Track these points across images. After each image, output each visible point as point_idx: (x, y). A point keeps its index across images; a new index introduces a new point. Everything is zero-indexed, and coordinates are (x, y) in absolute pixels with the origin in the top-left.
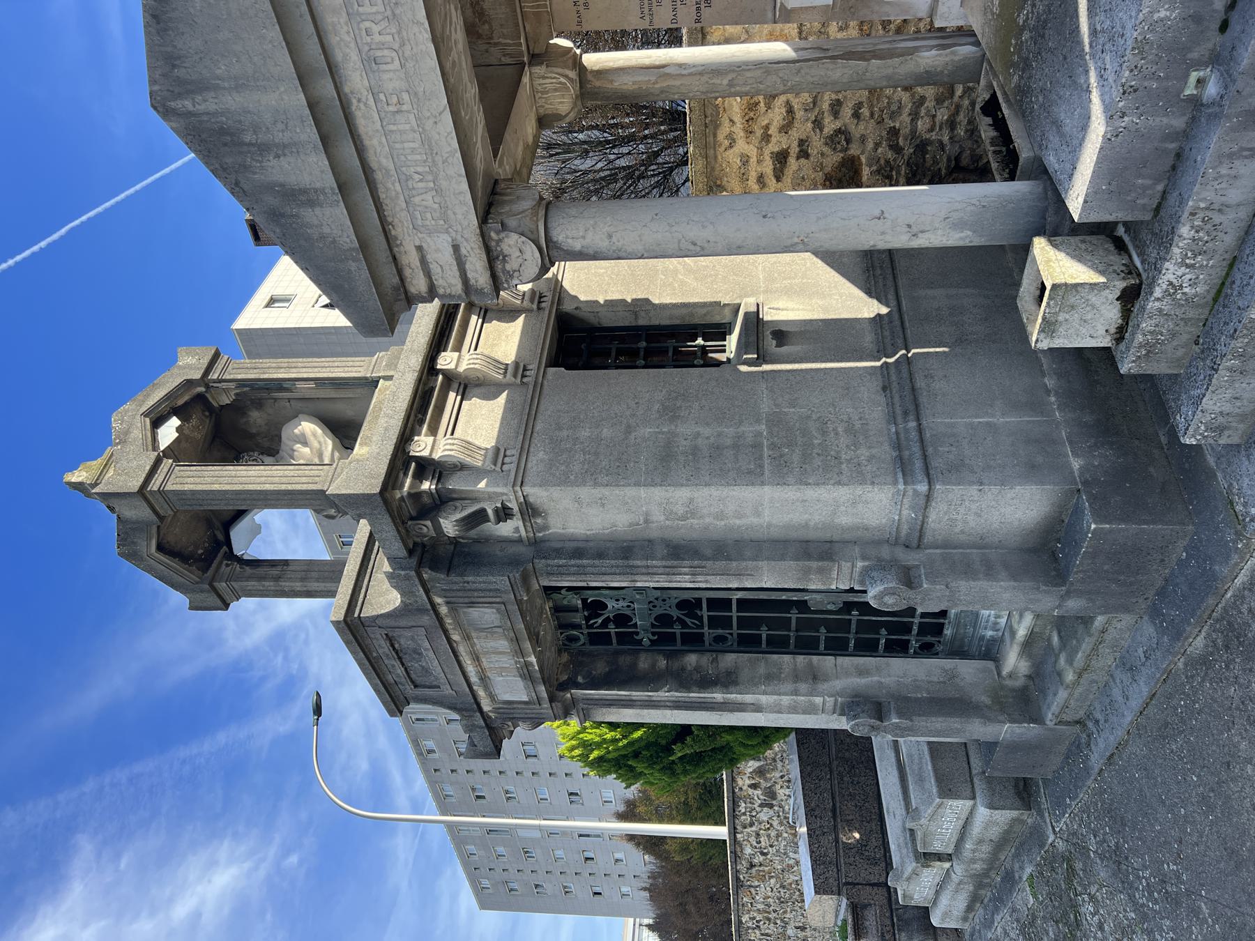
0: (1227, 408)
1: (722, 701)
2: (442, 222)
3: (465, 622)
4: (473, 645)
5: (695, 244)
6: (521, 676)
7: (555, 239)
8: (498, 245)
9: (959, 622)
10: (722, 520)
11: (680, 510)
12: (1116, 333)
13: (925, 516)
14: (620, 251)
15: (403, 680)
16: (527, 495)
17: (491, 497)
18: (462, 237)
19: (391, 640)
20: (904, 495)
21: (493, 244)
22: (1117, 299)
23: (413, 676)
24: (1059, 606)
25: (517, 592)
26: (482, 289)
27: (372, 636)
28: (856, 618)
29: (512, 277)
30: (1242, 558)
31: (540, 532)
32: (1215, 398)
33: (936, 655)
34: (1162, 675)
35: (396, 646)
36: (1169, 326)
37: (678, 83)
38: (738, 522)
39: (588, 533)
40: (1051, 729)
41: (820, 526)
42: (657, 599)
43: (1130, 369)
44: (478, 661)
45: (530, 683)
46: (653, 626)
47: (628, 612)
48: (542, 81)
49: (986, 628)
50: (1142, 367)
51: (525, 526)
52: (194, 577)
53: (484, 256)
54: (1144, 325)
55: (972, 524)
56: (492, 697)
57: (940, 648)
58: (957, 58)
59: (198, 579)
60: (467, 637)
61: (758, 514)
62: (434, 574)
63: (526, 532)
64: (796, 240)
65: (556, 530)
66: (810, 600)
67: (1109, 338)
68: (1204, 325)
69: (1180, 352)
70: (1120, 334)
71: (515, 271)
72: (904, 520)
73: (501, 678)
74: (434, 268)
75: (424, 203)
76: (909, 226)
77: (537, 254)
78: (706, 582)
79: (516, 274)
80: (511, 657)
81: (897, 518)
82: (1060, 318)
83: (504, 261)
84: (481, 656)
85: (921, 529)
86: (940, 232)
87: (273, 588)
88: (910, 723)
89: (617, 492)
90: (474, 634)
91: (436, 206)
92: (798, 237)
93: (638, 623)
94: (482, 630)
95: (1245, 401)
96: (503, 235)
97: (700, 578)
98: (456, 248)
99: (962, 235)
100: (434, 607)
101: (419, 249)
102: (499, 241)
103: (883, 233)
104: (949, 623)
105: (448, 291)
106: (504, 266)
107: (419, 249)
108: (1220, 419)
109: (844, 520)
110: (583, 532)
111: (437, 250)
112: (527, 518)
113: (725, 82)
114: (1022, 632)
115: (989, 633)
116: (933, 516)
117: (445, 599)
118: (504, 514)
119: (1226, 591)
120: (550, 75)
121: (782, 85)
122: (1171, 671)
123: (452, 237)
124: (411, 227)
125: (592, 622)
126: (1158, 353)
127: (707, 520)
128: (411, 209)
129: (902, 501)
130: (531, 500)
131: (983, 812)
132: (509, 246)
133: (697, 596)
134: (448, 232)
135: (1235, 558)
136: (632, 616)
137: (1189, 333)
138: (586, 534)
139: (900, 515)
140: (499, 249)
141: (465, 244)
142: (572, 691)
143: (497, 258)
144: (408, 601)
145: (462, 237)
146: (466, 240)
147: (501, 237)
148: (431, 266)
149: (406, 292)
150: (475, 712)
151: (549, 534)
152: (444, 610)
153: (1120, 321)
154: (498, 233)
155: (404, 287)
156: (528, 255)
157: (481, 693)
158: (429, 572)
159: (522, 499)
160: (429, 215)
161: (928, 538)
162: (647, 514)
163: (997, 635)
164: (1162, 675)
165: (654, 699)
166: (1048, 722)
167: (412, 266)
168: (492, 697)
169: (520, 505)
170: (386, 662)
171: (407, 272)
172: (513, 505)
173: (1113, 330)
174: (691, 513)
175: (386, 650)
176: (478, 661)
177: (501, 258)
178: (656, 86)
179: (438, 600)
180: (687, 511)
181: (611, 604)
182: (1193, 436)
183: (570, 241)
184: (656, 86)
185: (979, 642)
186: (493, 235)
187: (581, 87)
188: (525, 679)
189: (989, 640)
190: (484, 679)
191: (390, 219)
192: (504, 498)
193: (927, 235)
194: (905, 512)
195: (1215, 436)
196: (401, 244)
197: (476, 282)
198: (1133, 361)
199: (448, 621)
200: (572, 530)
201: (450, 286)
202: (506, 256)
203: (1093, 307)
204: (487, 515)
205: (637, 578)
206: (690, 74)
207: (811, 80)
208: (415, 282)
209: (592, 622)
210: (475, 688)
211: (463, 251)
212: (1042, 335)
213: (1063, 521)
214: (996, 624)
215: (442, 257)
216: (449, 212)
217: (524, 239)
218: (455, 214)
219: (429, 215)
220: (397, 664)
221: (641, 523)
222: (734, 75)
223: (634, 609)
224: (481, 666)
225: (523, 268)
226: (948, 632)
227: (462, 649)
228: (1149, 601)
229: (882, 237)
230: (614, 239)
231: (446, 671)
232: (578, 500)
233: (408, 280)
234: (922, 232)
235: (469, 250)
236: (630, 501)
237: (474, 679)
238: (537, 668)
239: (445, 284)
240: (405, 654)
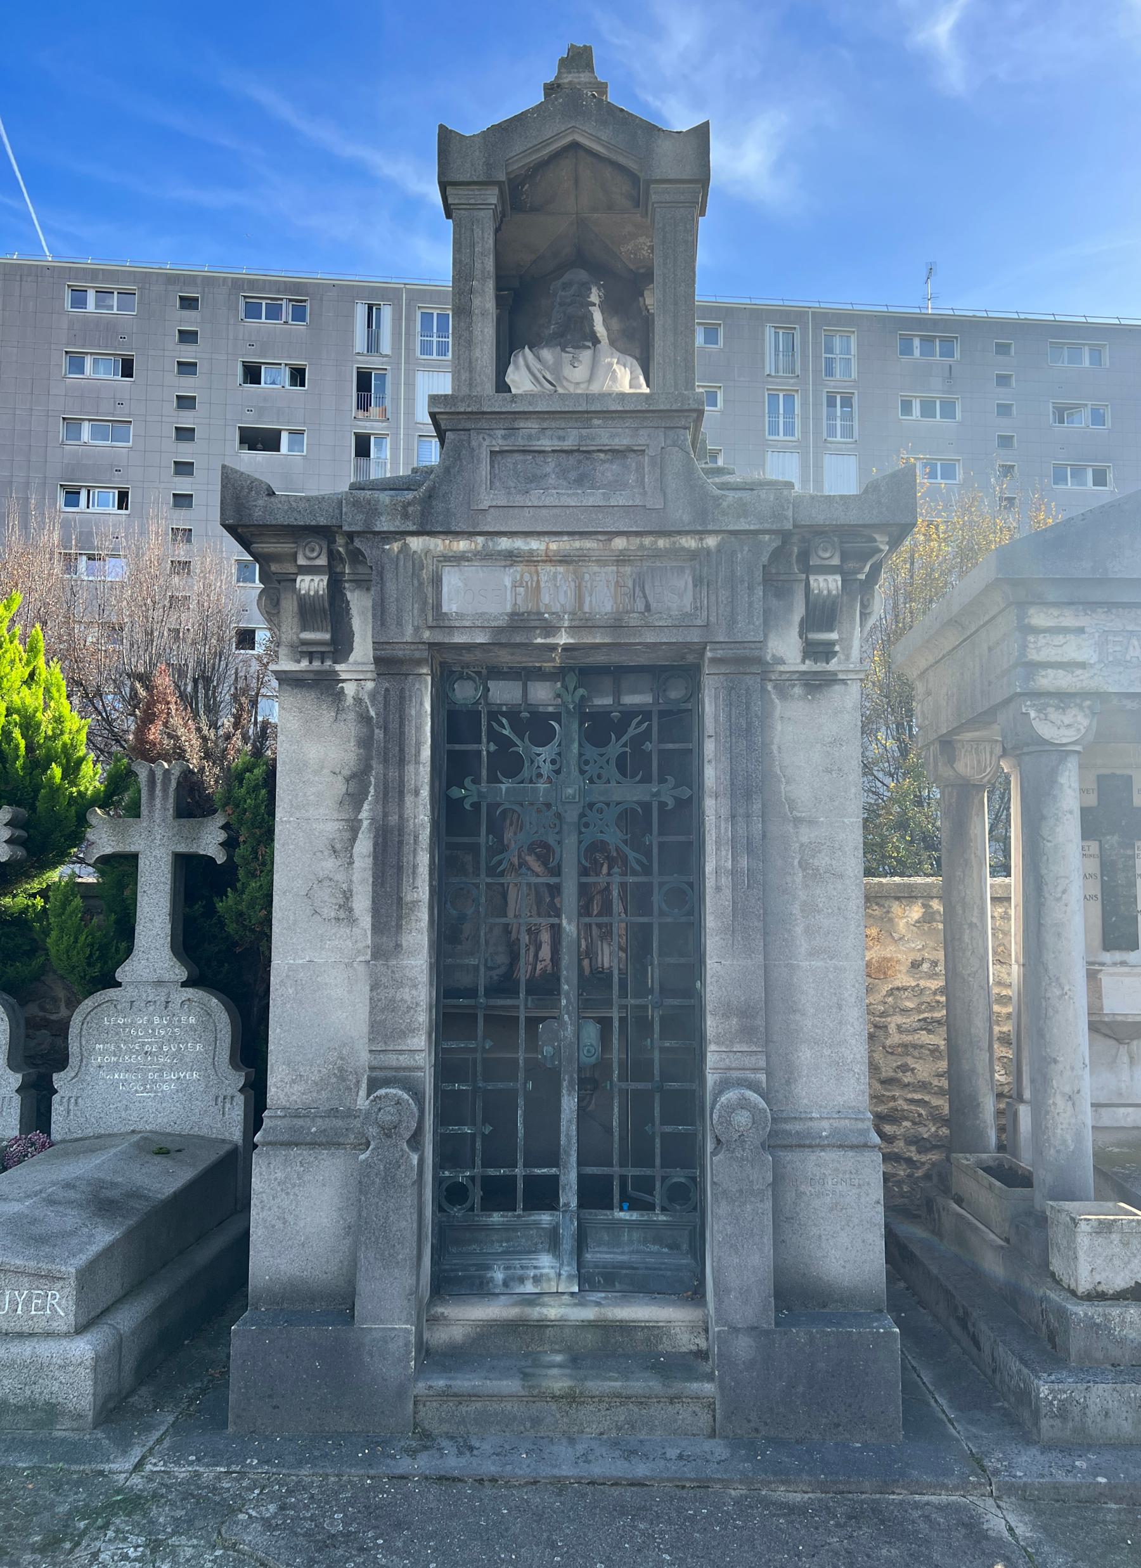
0: (1093, 1409)
1: (409, 898)
2: (1111, 659)
3: (658, 564)
4: (602, 562)
5: (1064, 892)
6: (513, 614)
7: (1069, 759)
8: (1076, 705)
9: (515, 1230)
10: (802, 911)
11: (822, 861)
12: (1097, 1292)
13: (823, 1148)
14: (1057, 820)
15: (520, 442)
16: (846, 684)
17: (846, 642)
18: (1095, 674)
19: (617, 454)
20: (856, 1119)
21: (1078, 701)
22: (1136, 1282)
23: (519, 457)
24: (735, 1330)
25: (724, 646)
26: (1034, 680)
27: (641, 432)
28: (519, 1086)
29: (1039, 711)
30: (956, 1488)
31: (775, 687)
32: (1106, 1394)
33: (439, 1208)
34: (692, 1480)
35: (602, 456)
36: (1131, 1334)
37: (975, 876)
38: (799, 930)
39: (775, 748)
40: (401, 1392)
41: (793, 1026)
42: (559, 816)
43: (1076, 1314)
44: (560, 561)
45: (500, 623)
46: (492, 807)
47: (526, 773)
48: (988, 749)
49: (507, 1268)
50: (1079, 1325)
51: (797, 672)
52: (515, 167)
53: (1073, 690)
54: (1132, 1311)
55: (816, 1203)
56: (459, 559)
57: (457, 1211)
58: (989, 1130)
59: (510, 170)
60: (622, 559)
61: (813, 954)
62: (770, 549)
63: (782, 672)
64: (1067, 988)
65: (779, 708)
66: (563, 1024)
67: (1089, 1287)
68: (1133, 1365)
69: (1099, 1355)
70: (1097, 1296)
71: (1046, 715)
72: (810, 1124)
73: (508, 583)
74: (1059, 639)
75: (1131, 648)
76: (1078, 1092)
77: (1065, 741)
78: (718, 889)
79: (1042, 716)
80: (568, 609)
81: (814, 1115)
82: (1114, 1236)
83: (1057, 708)
84: (571, 568)
85: (804, 1146)
86: (1073, 1121)
87: (478, 265)
88: (409, 1182)
89: (853, 790)
90: (628, 569)
91: (1128, 658)
92: (1070, 990)
93: (503, 787)
94: (640, 582)
95: (1103, 1423)
96: (1087, 712)
97: (725, 881)
98: (1083, 665)
99: (1070, 1141)
100: (702, 534)
101: (1081, 630)
102: (1081, 708)
103: (1072, 1068)
104: (519, 1216)
105: (1031, 646)
106: (1052, 706)
107: (1081, 630)
108: (1076, 1410)
109: (805, 1055)
110: (776, 740)
111: (1079, 647)
112: (808, 677)
113: (975, 920)
114: (552, 1312)
115: (499, 1276)
116: (829, 1156)
117: (713, 549)
118: (817, 651)
119: (893, 1493)
120: (993, 758)
121: (969, 972)
122: (708, 1487)
123: (1095, 664)
124: (1106, 629)
125: (504, 721)
126: (1097, 1333)
127: (802, 895)
128: (1125, 634)
129: (845, 1118)
130: (837, 687)
131: (83, 1349)
132: (1075, 716)
133: (565, 869)
134: (1100, 661)
135: (950, 1482)
136: (519, 778)
137: (1124, 1356)
138: (772, 743)
139: (822, 1118)
140: (1072, 705)
141: (1087, 675)
142: (429, 678)
143: (1062, 701)
144: (725, 504)
145: (1095, 674)
146: (1091, 677)
147: (1086, 709)
148: (1061, 636)
149: (1032, 603)
150: (422, 524)
151: (772, 702)
152: (690, 543)
153: (1111, 1292)
154: (1089, 707)
155: (1038, 604)
156: (1063, 731)
157: (462, 545)
158: (774, 545)
159: (841, 676)
160: (1118, 648)
161: (787, 1156)
162: (812, 822)
163: (495, 1286)
164: (692, 1480)
165: (409, 799)
166: (421, 1385)
167: (1062, 619)
168: (459, 559)
169: (835, 674)
170: (575, 432)
171: (1055, 612)
172: (833, 665)
173: (1100, 1288)
174: (815, 876)
175: (606, 441)
176: (560, 561)
177: (1062, 705)
178: (973, 856)
179: (711, 542)
180: (818, 870)
181: (545, 753)
182: (1052, 1391)
183: (1067, 773)
184: (973, 856)
185: (474, 1265)
186: (1088, 703)
187: (974, 785)
188: (511, 619)
189: (481, 1277)
190: (511, 558)
191: (1114, 611)
192: (841, 656)
193: (1069, 1108)
194: (825, 1124)
195: (1052, 1411)
196: (1086, 614)
197: (1043, 676)
198: (1086, 1315)
199: (661, 543)
200: (779, 728)
201: (1038, 650)
202: (1064, 710)
203: (1129, 1262)
204: (820, 629)
205: (725, 802)
206: (981, 887)
207: (974, 1000)
208: (1042, 615)
209: (504, 721)
210: (480, 540)
211: (1079, 672)
212: (1095, 1224)
213: (824, 1307)
214: (522, 1280)
215: (1073, 649)
216: (1122, 669)
217: (1083, 731)
218: (1120, 673)
219: (1118, 648)
220: (568, 444)
221: (795, 813)
222: (980, 928)
223: (531, 782)
224: (546, 561)
225: (1049, 724)
226: (496, 1218)
227: (589, 544)
228: (754, 1435)
229: (1068, 1067)
230: (1069, 816)
231: (544, 511)
232: (837, 742)
233: (1045, 610)
234: (1073, 1104)
235: (1081, 678)
236: (836, 803)
237: (504, 543)
238: (539, 640)
239: (1039, 644)
240: (580, 462)
